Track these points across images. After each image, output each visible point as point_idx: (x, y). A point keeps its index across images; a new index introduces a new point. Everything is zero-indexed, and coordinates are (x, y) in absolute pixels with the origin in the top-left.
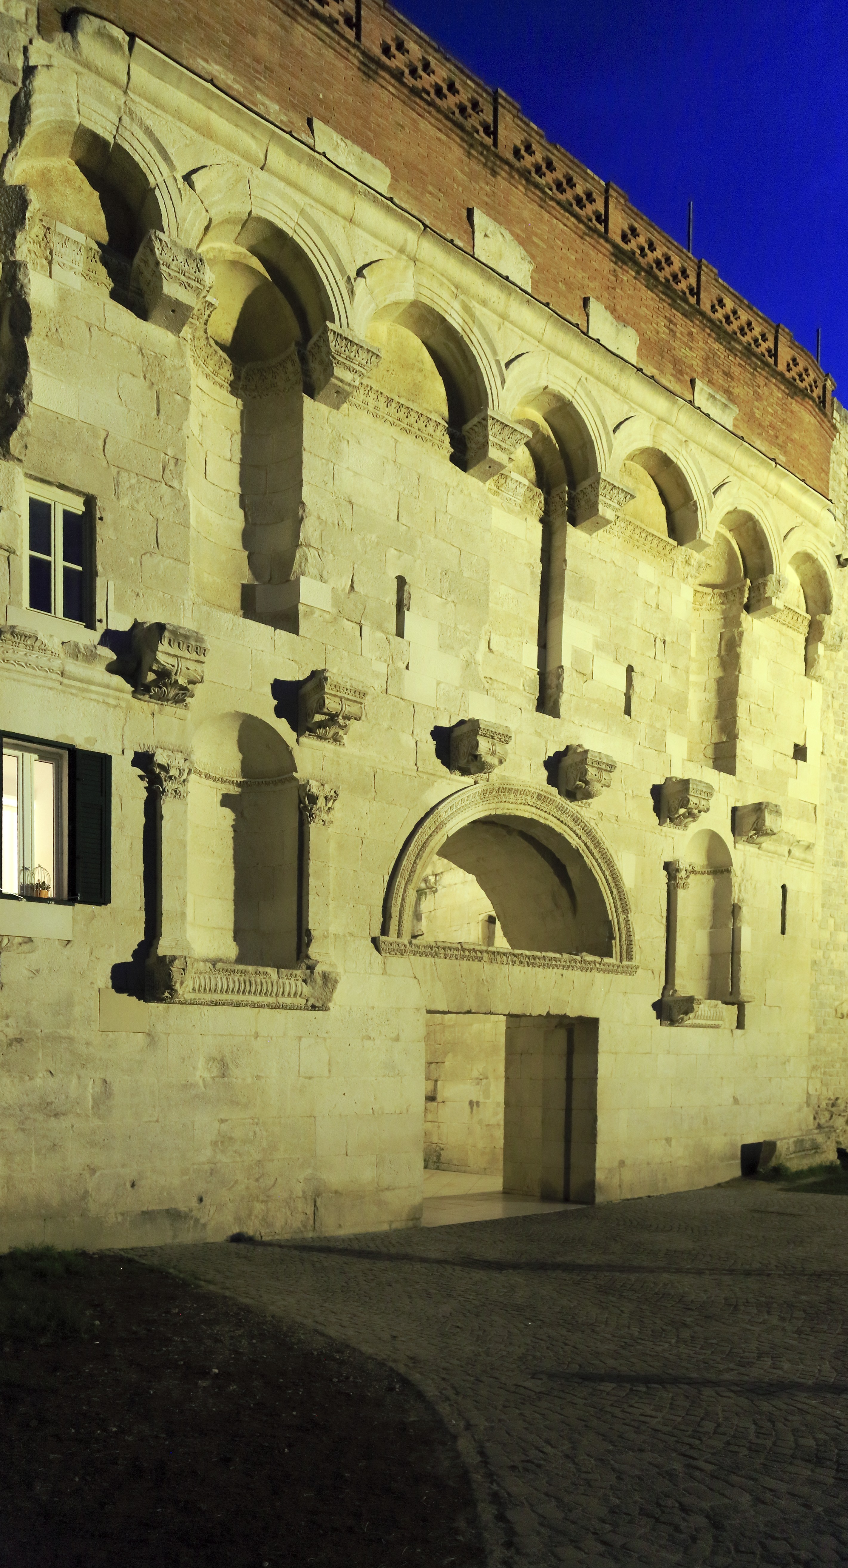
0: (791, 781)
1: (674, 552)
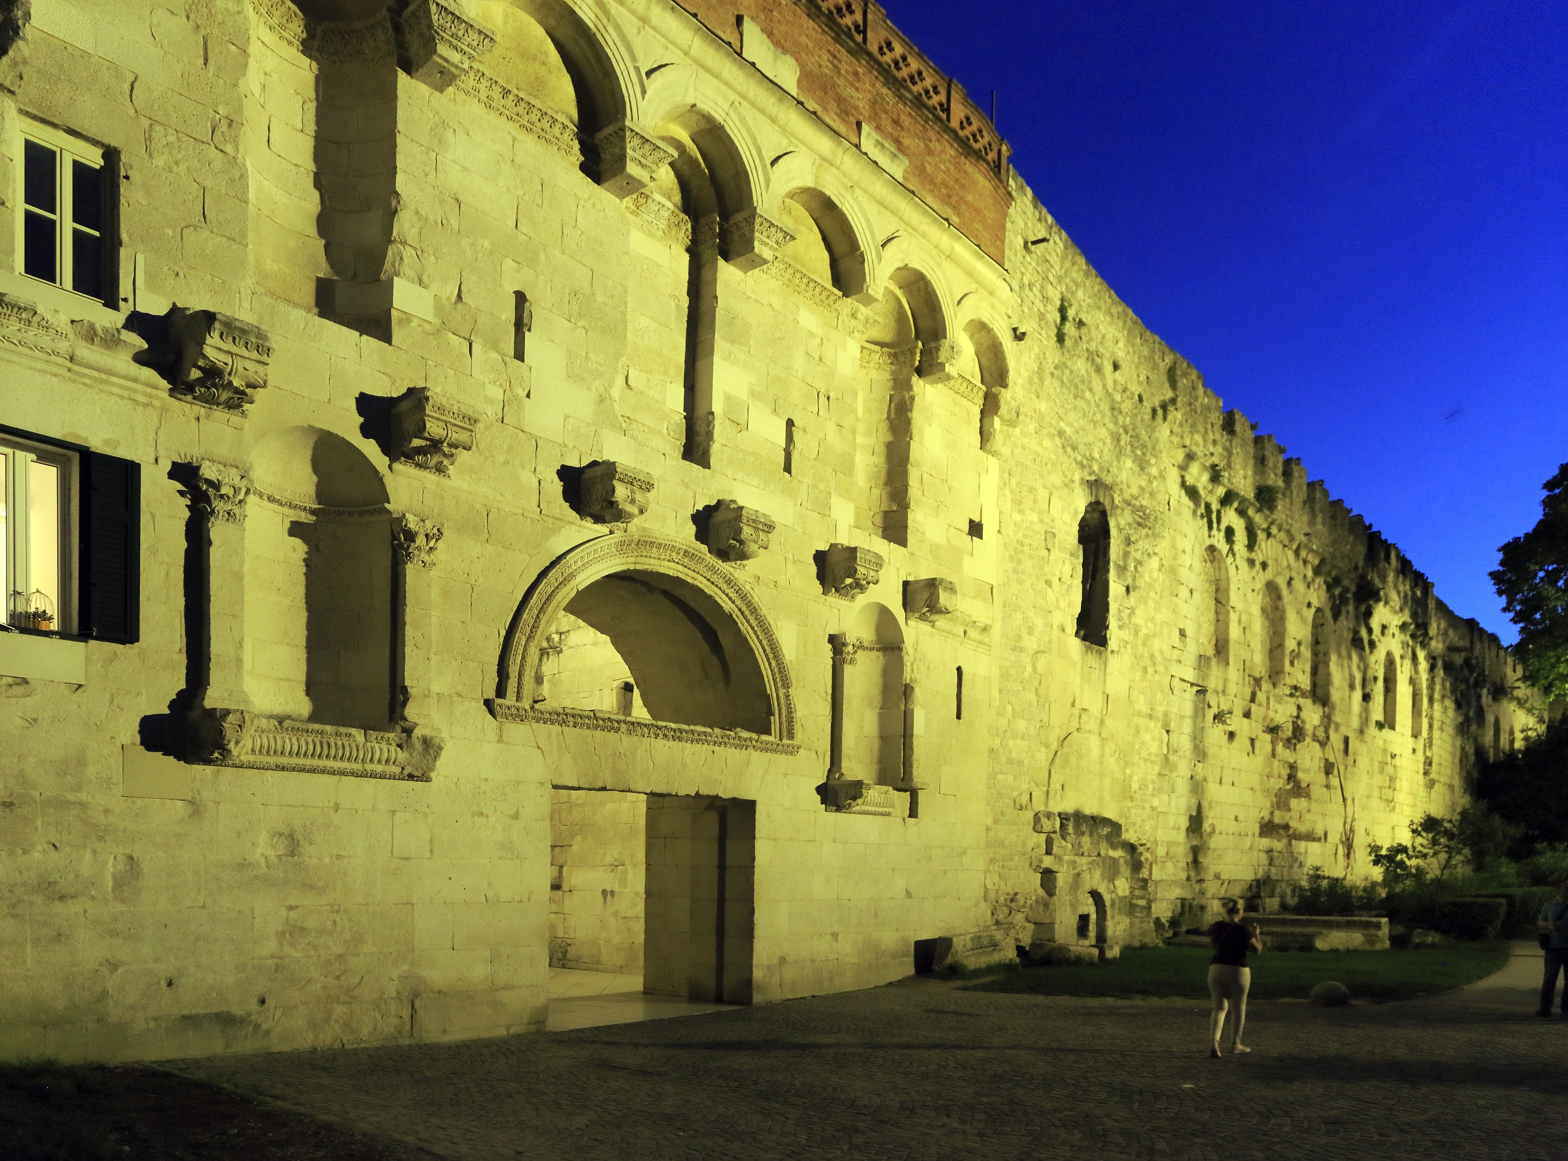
0: (967, 558)
1: (839, 303)
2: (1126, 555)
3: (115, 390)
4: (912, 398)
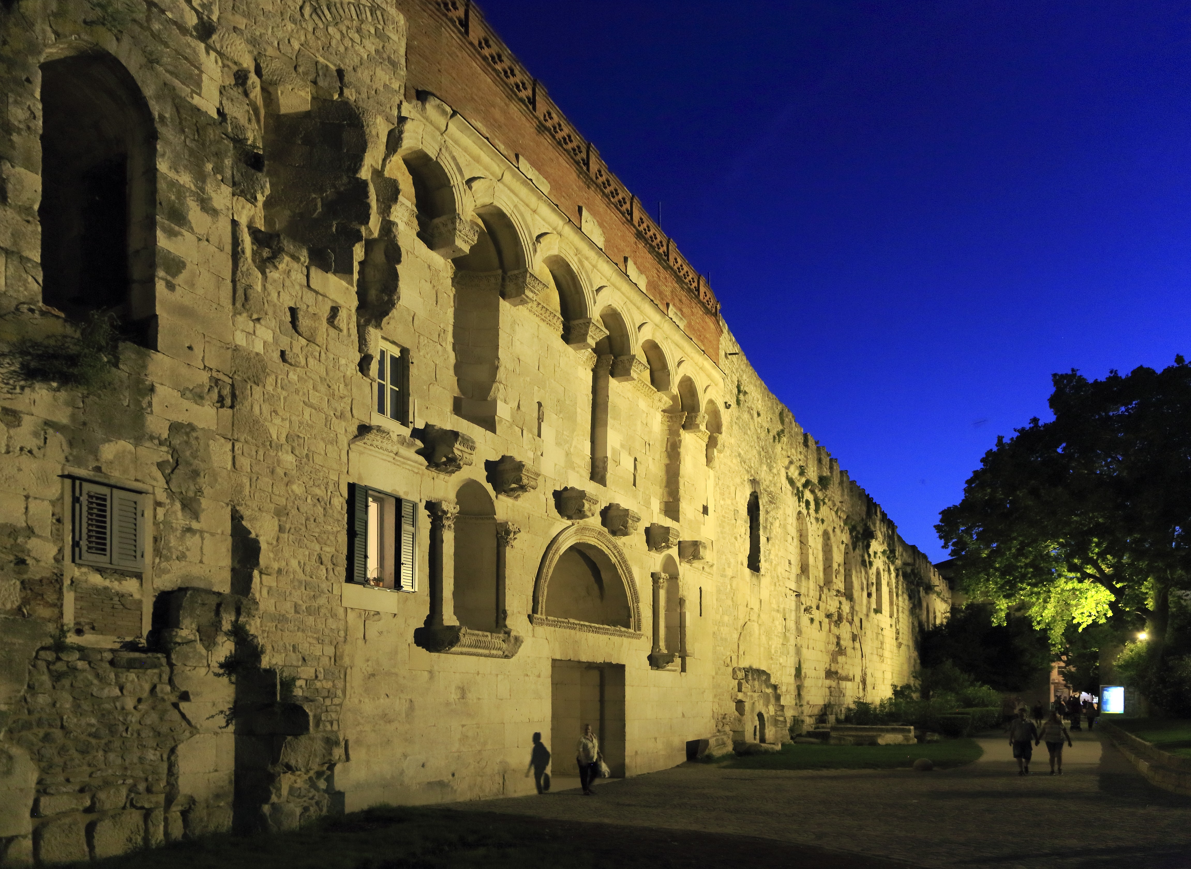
0: (702, 526)
2: (766, 519)
3: (408, 467)
4: (680, 441)
